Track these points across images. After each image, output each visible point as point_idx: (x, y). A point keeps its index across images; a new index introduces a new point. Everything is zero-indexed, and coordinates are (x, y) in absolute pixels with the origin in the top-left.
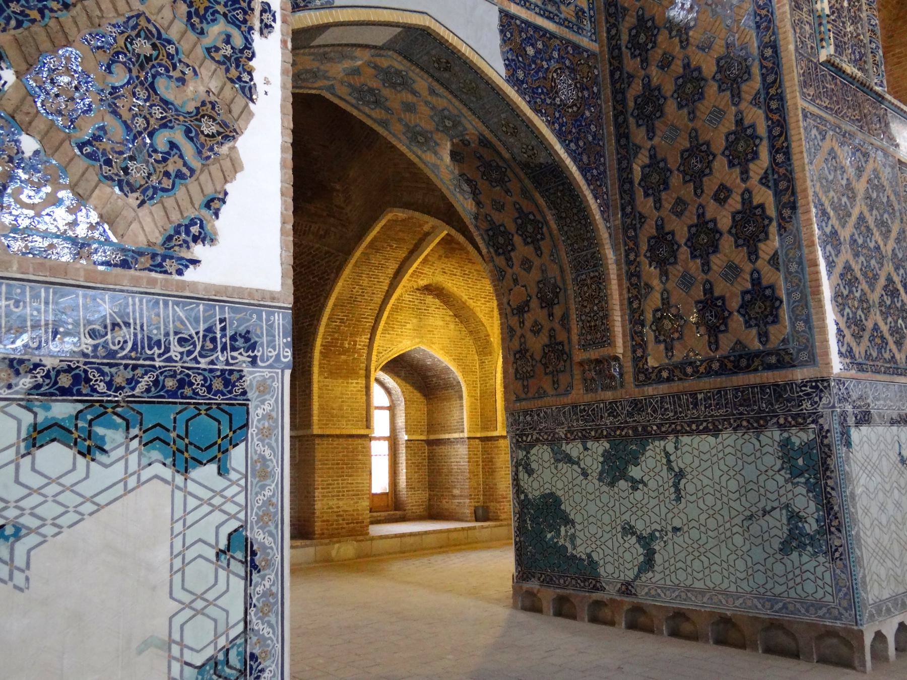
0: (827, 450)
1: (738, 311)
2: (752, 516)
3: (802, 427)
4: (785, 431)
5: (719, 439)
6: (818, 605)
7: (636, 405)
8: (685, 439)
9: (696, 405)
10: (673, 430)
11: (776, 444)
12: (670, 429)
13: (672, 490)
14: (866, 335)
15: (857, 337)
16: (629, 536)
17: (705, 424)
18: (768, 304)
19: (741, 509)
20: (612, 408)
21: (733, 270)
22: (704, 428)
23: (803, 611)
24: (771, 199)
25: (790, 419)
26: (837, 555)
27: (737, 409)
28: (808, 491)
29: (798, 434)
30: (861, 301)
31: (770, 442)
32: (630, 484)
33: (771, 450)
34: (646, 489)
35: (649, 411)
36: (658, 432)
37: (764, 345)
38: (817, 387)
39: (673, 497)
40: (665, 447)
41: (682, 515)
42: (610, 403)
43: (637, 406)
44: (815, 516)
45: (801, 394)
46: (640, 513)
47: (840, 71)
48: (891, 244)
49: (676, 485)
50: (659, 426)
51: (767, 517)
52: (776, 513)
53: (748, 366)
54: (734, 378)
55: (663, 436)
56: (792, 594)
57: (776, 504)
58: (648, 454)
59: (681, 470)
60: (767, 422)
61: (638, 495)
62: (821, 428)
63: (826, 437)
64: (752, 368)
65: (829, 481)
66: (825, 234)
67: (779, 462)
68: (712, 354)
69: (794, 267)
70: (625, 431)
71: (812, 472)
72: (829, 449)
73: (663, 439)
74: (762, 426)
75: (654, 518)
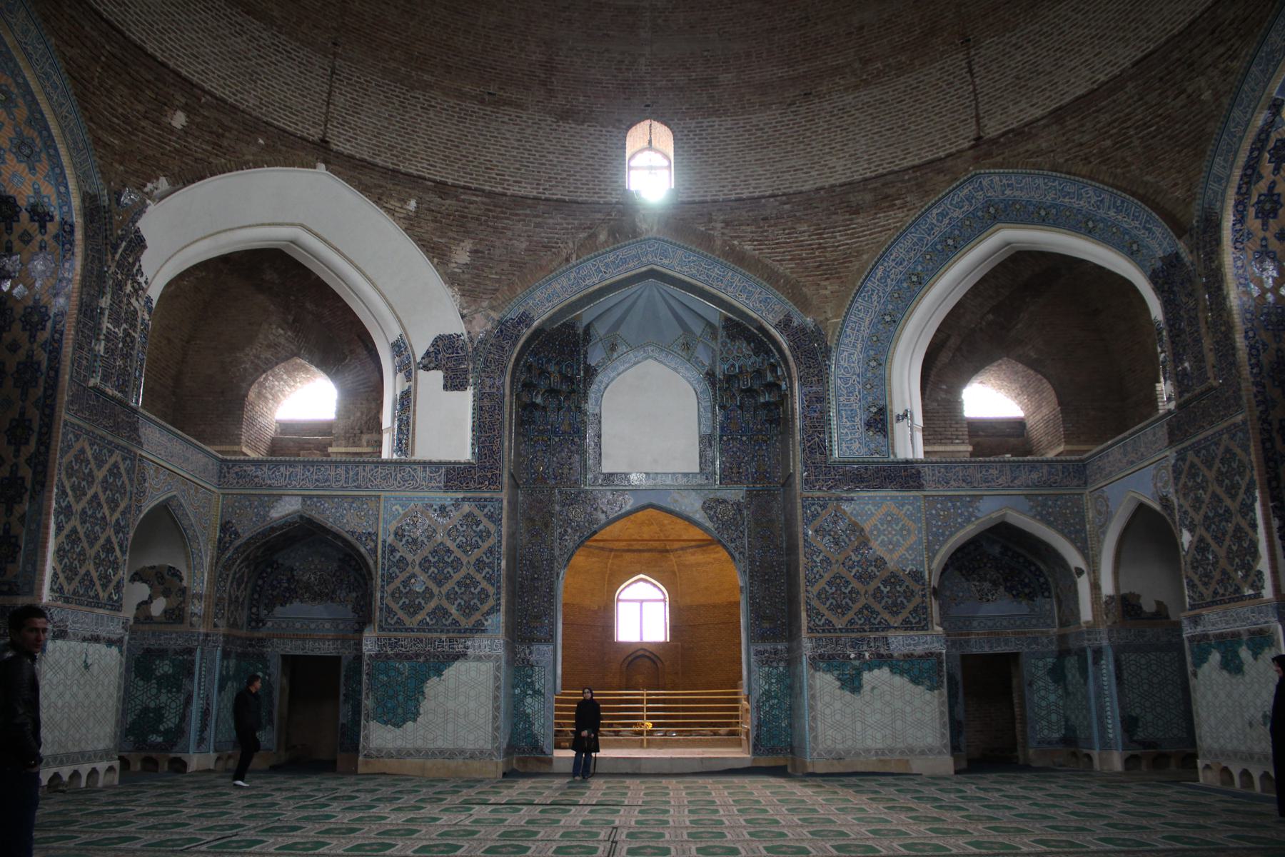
14: (78, 579)
15: (69, 580)
24: (30, 475)
30: (79, 554)
47: (104, 393)
48: (117, 515)
66: (60, 507)
69: (33, 527)
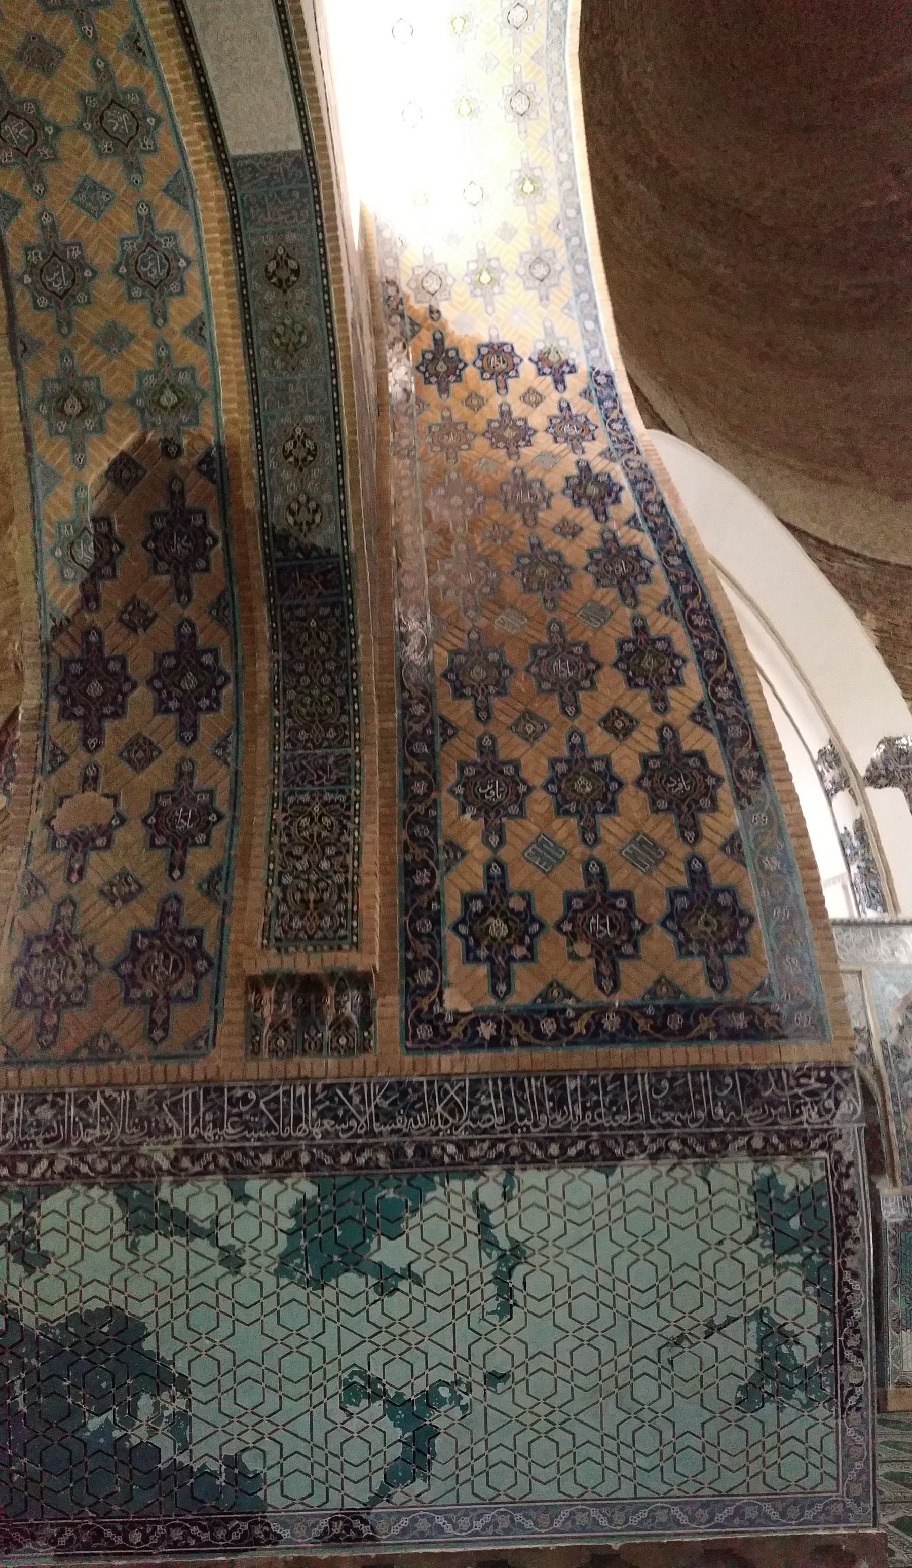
0: (848, 1201)
1: (663, 924)
2: (682, 1337)
3: (800, 1154)
4: (765, 1162)
5: (616, 1177)
6: (805, 1501)
7: (404, 1094)
8: (531, 1177)
9: (560, 1103)
10: (499, 1155)
11: (744, 1189)
12: (492, 1155)
13: (491, 1290)
16: (364, 1403)
17: (581, 1145)
18: (725, 919)
19: (658, 1324)
20: (332, 1100)
21: (647, 852)
22: (579, 1153)
23: (775, 1516)
25: (775, 1140)
26: (852, 1401)
27: (657, 1115)
28: (807, 1282)
29: (791, 1170)
31: (730, 1184)
32: (372, 1281)
33: (732, 1200)
34: (417, 1291)
35: (439, 1109)
36: (460, 1158)
37: (720, 992)
38: (829, 1080)
39: (492, 1305)
40: (476, 1194)
41: (512, 1345)
42: (326, 1087)
43: (404, 1096)
44: (817, 1331)
45: (800, 1092)
46: (397, 1347)
49: (502, 1281)
50: (462, 1147)
51: (715, 1338)
52: (735, 1330)
53: (685, 1030)
54: (654, 1051)
55: (470, 1168)
56: (757, 1486)
57: (735, 1312)
58: (427, 1210)
59: (516, 1246)
60: (725, 1144)
61: (396, 1304)
62: (839, 1156)
63: (847, 1176)
64: (694, 1033)
65: (848, 1259)
67: (749, 1227)
68: (604, 998)
70: (366, 1154)
71: (816, 1241)
72: (853, 1199)
73: (472, 1175)
74: (714, 1152)
75: (436, 1355)
